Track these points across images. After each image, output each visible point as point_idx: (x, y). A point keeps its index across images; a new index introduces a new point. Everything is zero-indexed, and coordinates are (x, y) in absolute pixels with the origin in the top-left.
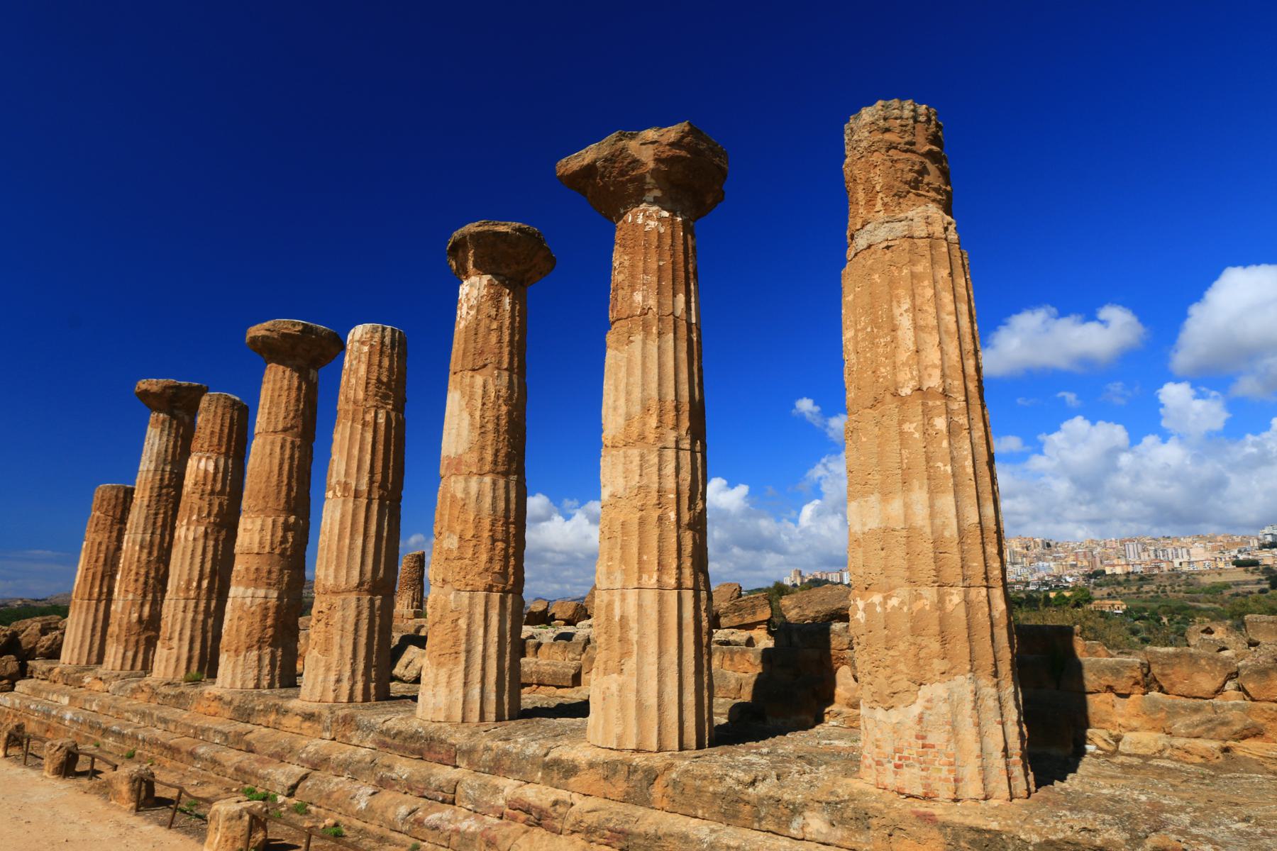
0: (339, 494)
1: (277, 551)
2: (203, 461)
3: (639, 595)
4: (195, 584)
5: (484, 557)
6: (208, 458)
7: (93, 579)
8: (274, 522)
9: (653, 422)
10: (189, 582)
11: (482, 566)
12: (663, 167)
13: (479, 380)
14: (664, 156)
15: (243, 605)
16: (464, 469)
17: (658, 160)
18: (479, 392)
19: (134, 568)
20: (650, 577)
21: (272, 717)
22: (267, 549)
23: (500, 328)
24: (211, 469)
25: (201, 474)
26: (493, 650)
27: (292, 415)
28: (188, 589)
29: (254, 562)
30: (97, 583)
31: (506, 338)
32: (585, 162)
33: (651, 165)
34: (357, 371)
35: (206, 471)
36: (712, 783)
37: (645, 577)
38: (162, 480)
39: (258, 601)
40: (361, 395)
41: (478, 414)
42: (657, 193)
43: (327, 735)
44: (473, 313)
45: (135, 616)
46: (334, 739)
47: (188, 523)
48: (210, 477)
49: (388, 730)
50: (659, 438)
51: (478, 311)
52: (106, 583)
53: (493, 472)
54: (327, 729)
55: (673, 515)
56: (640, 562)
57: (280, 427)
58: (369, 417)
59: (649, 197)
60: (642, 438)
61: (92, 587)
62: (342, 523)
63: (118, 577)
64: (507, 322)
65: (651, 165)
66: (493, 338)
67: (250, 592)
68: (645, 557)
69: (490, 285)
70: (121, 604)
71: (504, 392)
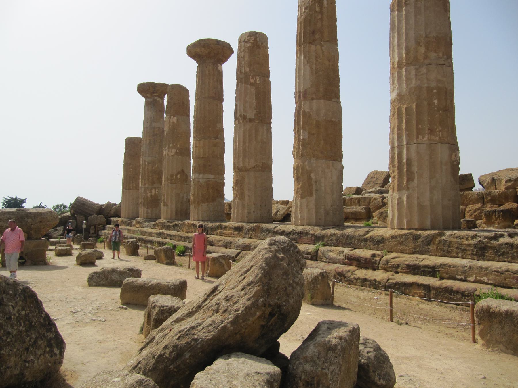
0: (241, 121)
3: (417, 147)
5: (322, 142)
6: (174, 116)
9: (422, 50)
10: (172, 176)
13: (313, 47)
15: (199, 182)
19: (146, 173)
20: (423, 137)
28: (172, 180)
34: (244, 57)
35: (173, 122)
36: (467, 239)
37: (420, 137)
38: (154, 132)
40: (247, 69)
41: (314, 66)
43: (247, 236)
45: (149, 194)
46: (250, 238)
47: (169, 148)
49: (277, 230)
50: (426, 57)
51: (310, 10)
54: (246, 233)
55: (436, 102)
56: (417, 129)
60: (416, 59)
62: (244, 136)
63: (140, 177)
67: (201, 176)
68: (420, 126)
70: (143, 189)
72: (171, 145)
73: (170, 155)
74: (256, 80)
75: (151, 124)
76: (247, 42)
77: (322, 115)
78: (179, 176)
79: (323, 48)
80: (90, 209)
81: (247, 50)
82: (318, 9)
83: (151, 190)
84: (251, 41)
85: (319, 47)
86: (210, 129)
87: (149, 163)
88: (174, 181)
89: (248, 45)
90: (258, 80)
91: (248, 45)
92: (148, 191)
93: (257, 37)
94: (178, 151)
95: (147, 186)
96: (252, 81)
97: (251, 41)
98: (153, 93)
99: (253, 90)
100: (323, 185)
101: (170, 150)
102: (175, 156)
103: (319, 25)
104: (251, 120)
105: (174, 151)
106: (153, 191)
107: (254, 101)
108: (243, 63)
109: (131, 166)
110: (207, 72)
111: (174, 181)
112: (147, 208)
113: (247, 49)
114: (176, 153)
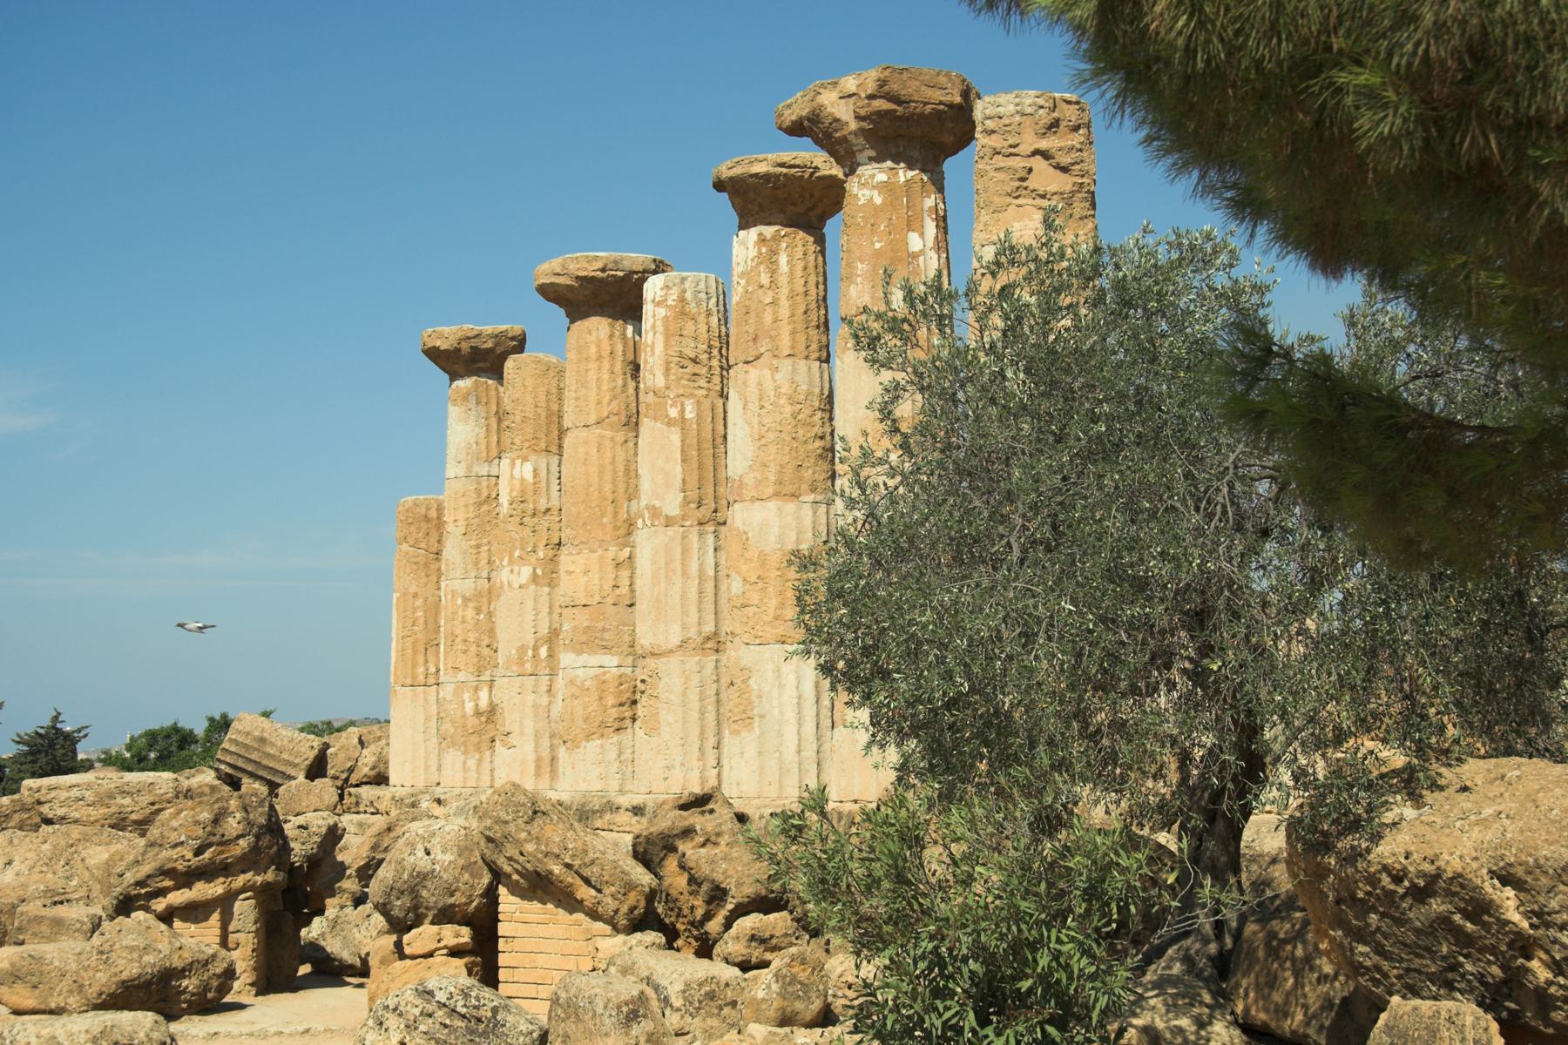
1: (610, 600)
2: (518, 462)
4: (530, 653)
6: (525, 459)
7: (415, 652)
8: (601, 557)
11: (771, 612)
12: (864, 124)
14: (862, 112)
16: (748, 494)
17: (858, 117)
18: (752, 391)
21: (608, 816)
22: (597, 598)
23: (774, 303)
24: (529, 477)
25: (517, 484)
26: (790, 715)
27: (605, 401)
28: (521, 661)
29: (583, 618)
30: (421, 659)
31: (784, 312)
32: (794, 118)
33: (853, 125)
35: (522, 480)
38: (478, 492)
39: (593, 672)
40: (660, 381)
41: (755, 420)
42: (872, 153)
44: (743, 282)
45: (469, 707)
47: (511, 562)
48: (531, 487)
51: (748, 283)
52: (431, 658)
53: (777, 494)
57: (592, 419)
58: (673, 413)
59: (862, 157)
61: (414, 666)
64: (785, 291)
65: (853, 125)
66: (768, 318)
67: (584, 659)
69: (762, 240)
71: (786, 388)
72: (517, 553)
73: (516, 585)
74: (683, 411)
75: (469, 468)
76: (658, 304)
77: (772, 538)
78: (543, 652)
79: (778, 376)
80: (285, 756)
81: (660, 328)
82: (765, 279)
83: (476, 689)
84: (670, 302)
85: (767, 373)
86: (605, 520)
87: (466, 600)
88: (528, 666)
89: (662, 312)
90: (689, 408)
91: (662, 312)
92: (466, 696)
93: (684, 291)
94: (539, 572)
95: (461, 676)
96: (673, 413)
97: (670, 302)
98: (474, 361)
99: (675, 437)
100: (775, 703)
101: (516, 569)
102: (532, 587)
103: (768, 318)
104: (669, 522)
105: (526, 571)
106: (484, 694)
107: (679, 469)
108: (650, 360)
109: (419, 602)
110: (593, 349)
111: (528, 666)
112: (465, 752)
113: (659, 323)
114: (535, 578)
